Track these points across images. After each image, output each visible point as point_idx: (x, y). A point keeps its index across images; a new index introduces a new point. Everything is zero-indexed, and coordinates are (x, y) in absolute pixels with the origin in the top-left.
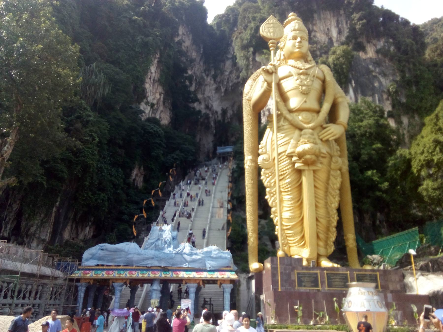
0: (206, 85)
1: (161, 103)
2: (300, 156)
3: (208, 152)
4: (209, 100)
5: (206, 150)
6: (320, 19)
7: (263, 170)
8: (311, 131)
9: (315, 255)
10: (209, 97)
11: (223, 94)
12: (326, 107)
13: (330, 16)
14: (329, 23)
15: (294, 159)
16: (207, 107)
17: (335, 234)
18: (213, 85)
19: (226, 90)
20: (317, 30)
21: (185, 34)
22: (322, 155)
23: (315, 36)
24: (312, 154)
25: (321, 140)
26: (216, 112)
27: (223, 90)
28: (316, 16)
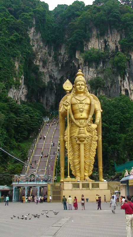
0: (50, 62)
1: (23, 84)
2: (79, 139)
3: (52, 105)
4: (52, 72)
5: (51, 104)
6: (111, 34)
7: (66, 142)
8: (83, 128)
9: (83, 176)
10: (51, 70)
11: (60, 68)
12: (91, 116)
13: (117, 32)
14: (116, 37)
15: (77, 139)
16: (51, 77)
17: (93, 167)
18: (54, 62)
19: (62, 65)
20: (110, 41)
21: (35, 32)
22: (87, 137)
23: (108, 45)
24: (83, 138)
25: (87, 131)
26: (57, 79)
27: (60, 66)
28: (109, 32)
